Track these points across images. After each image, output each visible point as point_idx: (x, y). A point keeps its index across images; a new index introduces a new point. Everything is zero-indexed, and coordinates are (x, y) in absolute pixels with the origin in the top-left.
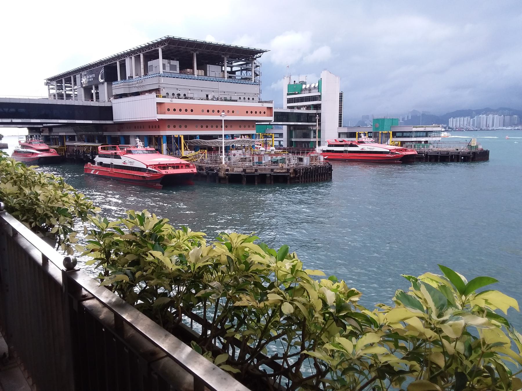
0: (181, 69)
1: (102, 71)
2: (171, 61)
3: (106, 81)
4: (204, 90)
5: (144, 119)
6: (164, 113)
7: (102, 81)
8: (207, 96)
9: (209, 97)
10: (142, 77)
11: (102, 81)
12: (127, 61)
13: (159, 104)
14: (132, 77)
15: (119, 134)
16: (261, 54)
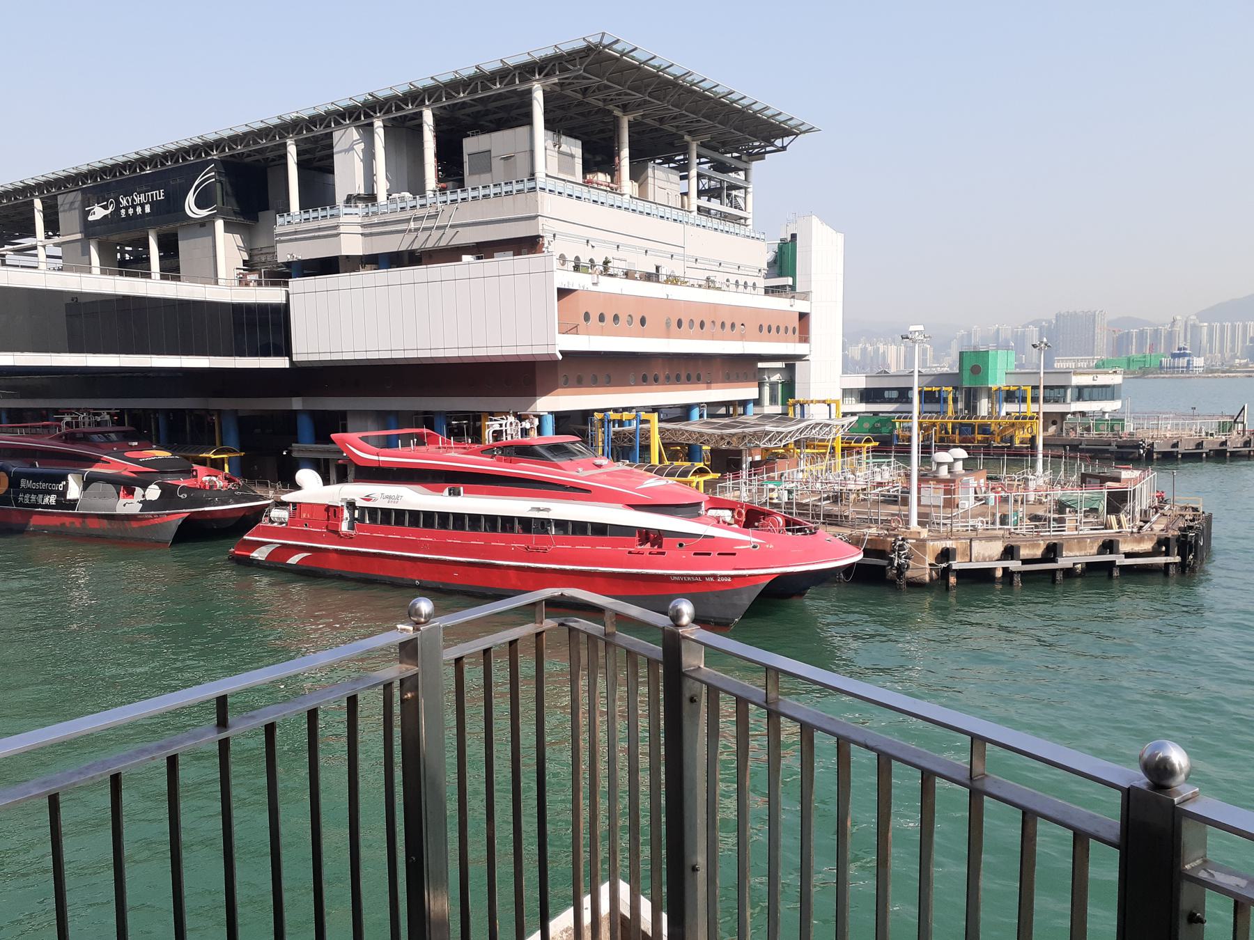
0: (587, 168)
1: (208, 176)
2: (563, 138)
3: (220, 213)
6: (573, 330)
7: (204, 213)
10: (429, 194)
11: (204, 213)
12: (347, 140)
13: (563, 293)
14: (371, 198)
15: (297, 404)
16: (787, 140)
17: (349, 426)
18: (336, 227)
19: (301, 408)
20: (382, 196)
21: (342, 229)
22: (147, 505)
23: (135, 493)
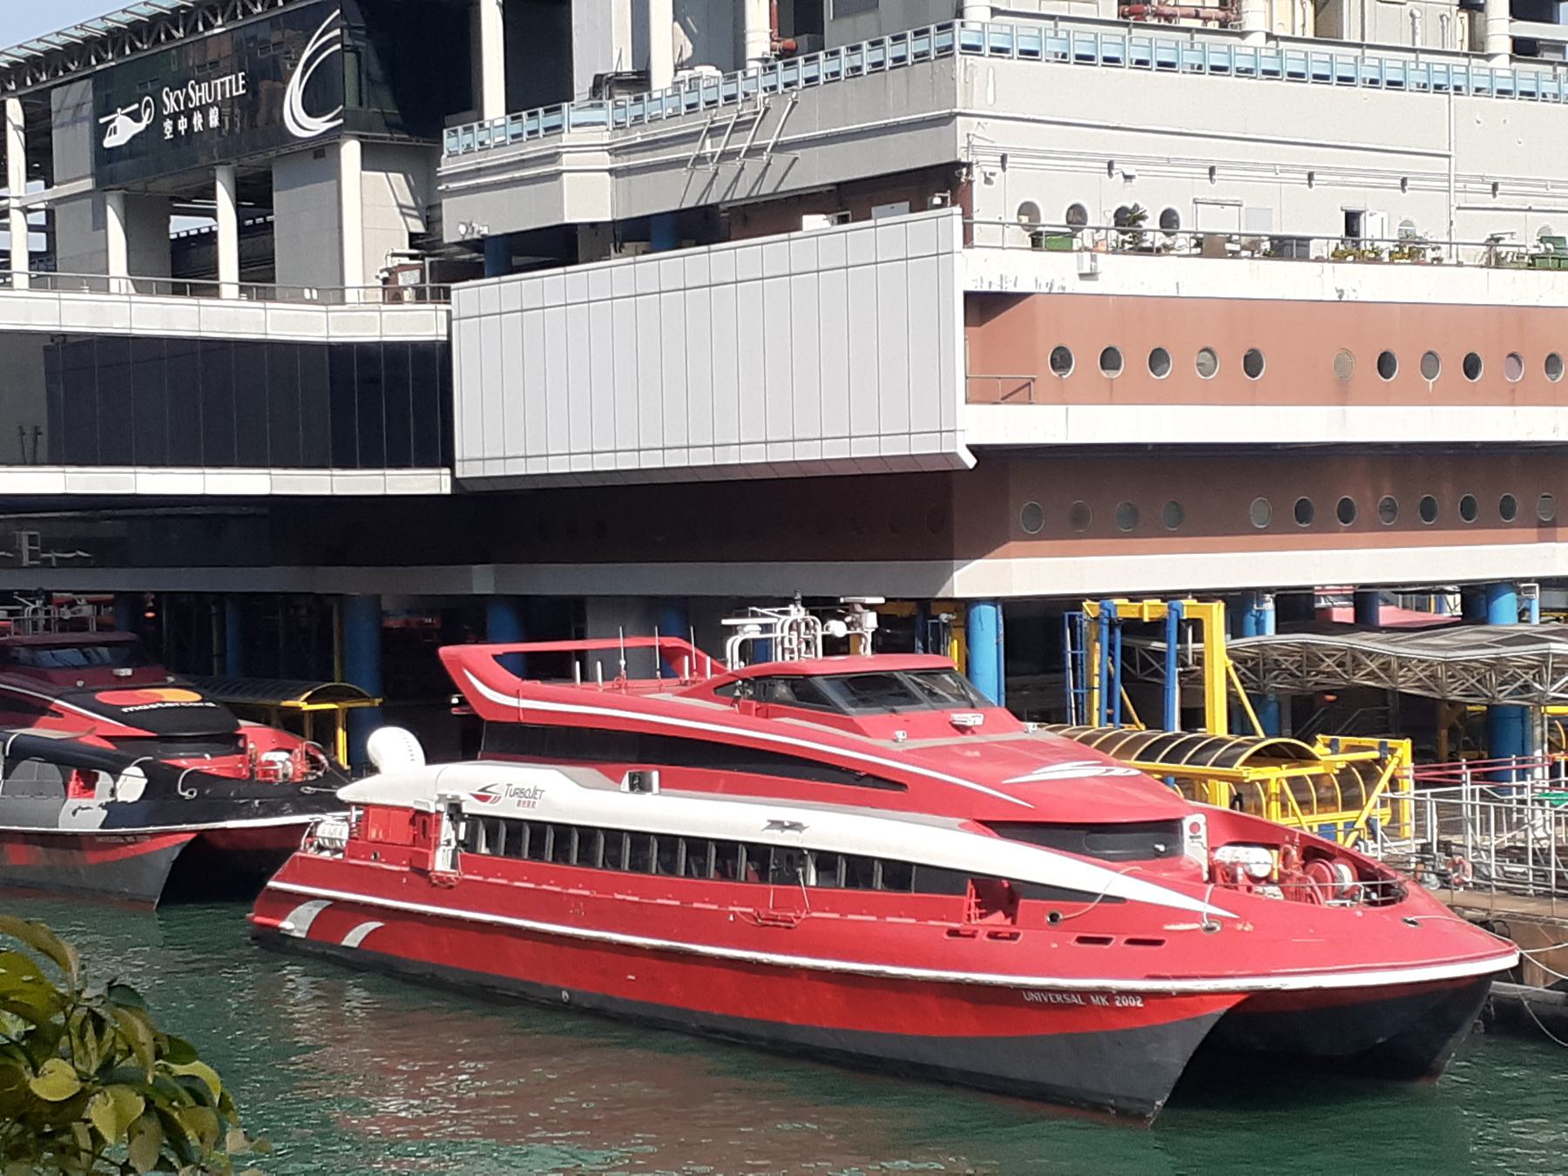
4: (1337, 171)
5: (731, 457)
8: (1352, 219)
9: (1370, 228)
14: (639, 81)
17: (589, 632)
18: (554, 157)
19: (491, 592)
20: (662, 76)
21: (567, 162)
22: (116, 812)
23: (98, 784)
